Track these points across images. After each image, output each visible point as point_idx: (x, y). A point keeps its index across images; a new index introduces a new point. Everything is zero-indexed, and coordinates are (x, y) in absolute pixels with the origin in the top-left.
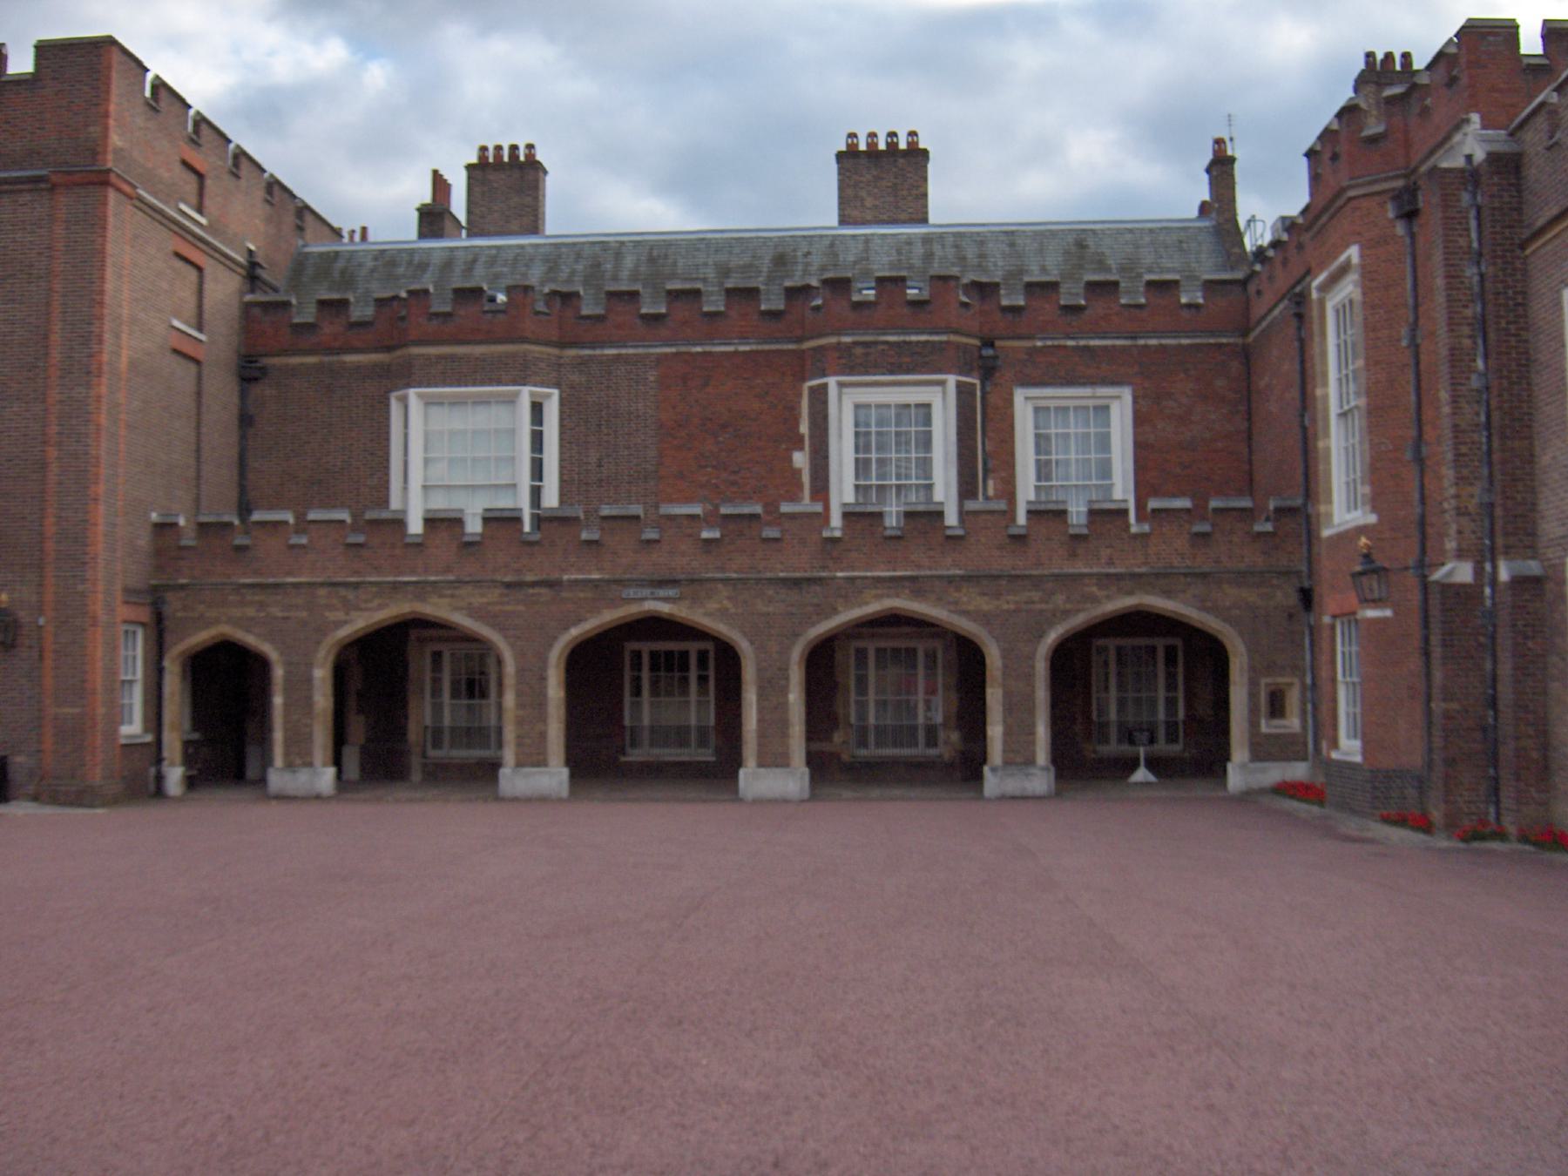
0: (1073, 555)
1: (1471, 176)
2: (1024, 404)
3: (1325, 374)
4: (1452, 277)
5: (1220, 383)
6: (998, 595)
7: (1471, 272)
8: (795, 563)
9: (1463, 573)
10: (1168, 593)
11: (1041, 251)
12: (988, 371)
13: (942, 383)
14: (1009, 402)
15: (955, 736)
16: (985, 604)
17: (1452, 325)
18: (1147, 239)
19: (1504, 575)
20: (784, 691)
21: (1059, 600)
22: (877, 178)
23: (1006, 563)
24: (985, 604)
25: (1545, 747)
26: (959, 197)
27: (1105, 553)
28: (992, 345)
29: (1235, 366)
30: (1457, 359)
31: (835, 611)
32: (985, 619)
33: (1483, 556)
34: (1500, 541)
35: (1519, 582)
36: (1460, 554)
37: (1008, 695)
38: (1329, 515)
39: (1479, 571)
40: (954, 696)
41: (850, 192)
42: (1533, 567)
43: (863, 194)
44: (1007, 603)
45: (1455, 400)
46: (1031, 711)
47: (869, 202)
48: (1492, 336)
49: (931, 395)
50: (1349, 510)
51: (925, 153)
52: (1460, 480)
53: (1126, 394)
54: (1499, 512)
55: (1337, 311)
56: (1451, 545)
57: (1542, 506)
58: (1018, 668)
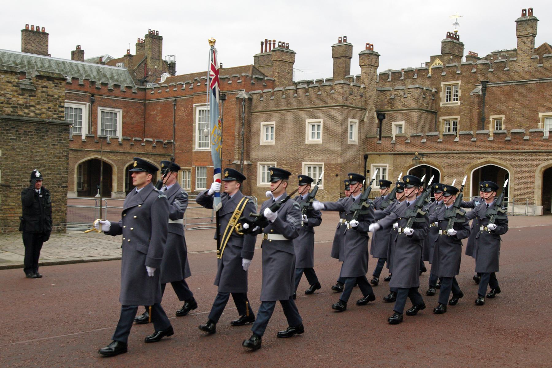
0: (131, 149)
1: (244, 100)
2: (100, 110)
3: (195, 121)
4: (240, 116)
5: (139, 111)
6: (117, 156)
7: (242, 115)
8: (76, 146)
9: (239, 162)
10: (148, 158)
11: (91, 70)
12: (92, 102)
13: (85, 104)
14: (97, 110)
15: (86, 185)
16: (115, 158)
17: (239, 123)
18: (114, 72)
19: (246, 163)
20: (73, 174)
21: (128, 158)
22: (35, 39)
23: (118, 149)
24: (115, 158)
25: (251, 190)
26: (59, 50)
27: (137, 149)
28: (93, 96)
29: (143, 107)
30: (240, 129)
31: (84, 157)
32: (114, 161)
33: (242, 160)
34: (245, 158)
35: (249, 165)
36: (238, 159)
37: (118, 177)
38: (195, 147)
39: (241, 162)
40: (86, 176)
41: (28, 41)
42: (250, 163)
43: (31, 42)
44: (119, 158)
45: (239, 135)
46: (122, 181)
47: (33, 45)
48: (246, 126)
49: (83, 107)
50: (200, 147)
51: (48, 34)
52: (239, 148)
53: (121, 111)
54: (245, 153)
55: (200, 111)
56: (236, 158)
57: (251, 153)
58: (120, 172)
